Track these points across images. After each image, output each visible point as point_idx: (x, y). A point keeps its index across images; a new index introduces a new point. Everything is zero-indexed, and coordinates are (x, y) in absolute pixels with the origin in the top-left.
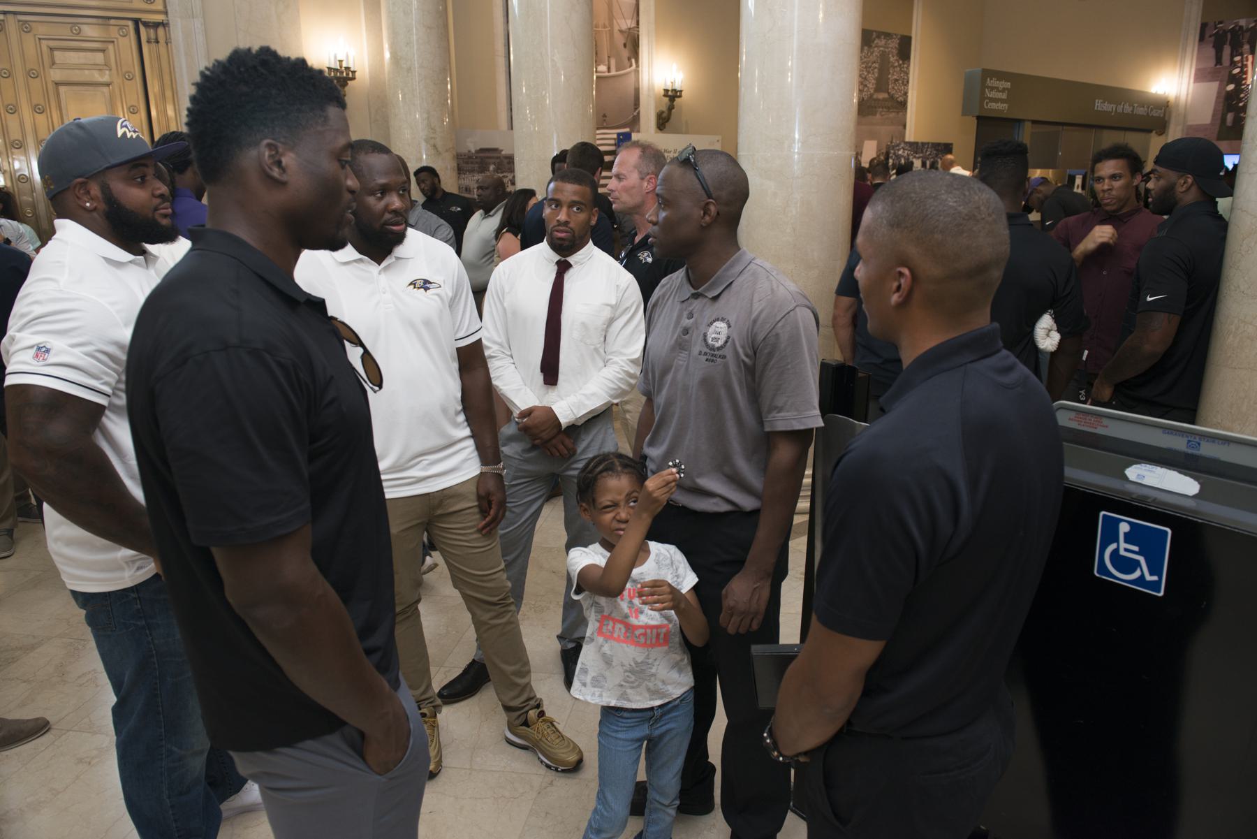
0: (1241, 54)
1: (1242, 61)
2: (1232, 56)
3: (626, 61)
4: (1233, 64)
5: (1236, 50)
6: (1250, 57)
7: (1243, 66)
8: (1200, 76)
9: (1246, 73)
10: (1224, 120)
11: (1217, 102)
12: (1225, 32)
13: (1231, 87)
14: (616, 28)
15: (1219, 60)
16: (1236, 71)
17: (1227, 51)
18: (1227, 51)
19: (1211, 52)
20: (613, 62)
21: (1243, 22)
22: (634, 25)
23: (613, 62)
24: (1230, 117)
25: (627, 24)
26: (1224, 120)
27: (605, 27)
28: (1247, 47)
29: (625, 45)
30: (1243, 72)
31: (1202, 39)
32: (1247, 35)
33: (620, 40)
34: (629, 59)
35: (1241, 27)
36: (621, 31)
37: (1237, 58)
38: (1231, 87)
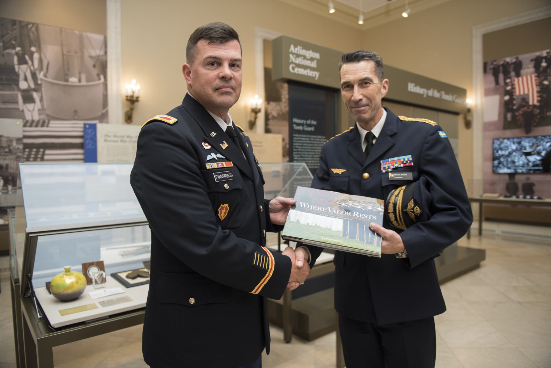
0: (510, 78)
1: (511, 82)
2: (505, 79)
3: (95, 77)
4: (506, 84)
5: (507, 75)
6: (516, 79)
7: (513, 85)
8: (488, 93)
9: (515, 88)
10: (505, 117)
11: (500, 107)
12: (498, 66)
13: (507, 98)
14: (86, 54)
15: (497, 82)
16: (509, 88)
17: (501, 77)
18: (501, 77)
19: (491, 78)
20: (83, 77)
21: (508, 60)
22: (102, 53)
23: (83, 77)
24: (509, 116)
25: (98, 52)
26: (505, 117)
27: (76, 52)
28: (513, 74)
29: (94, 66)
30: (513, 88)
31: (485, 71)
32: (512, 67)
33: (90, 63)
34: (98, 75)
35: (508, 63)
36: (91, 57)
37: (508, 81)
38: (507, 98)
